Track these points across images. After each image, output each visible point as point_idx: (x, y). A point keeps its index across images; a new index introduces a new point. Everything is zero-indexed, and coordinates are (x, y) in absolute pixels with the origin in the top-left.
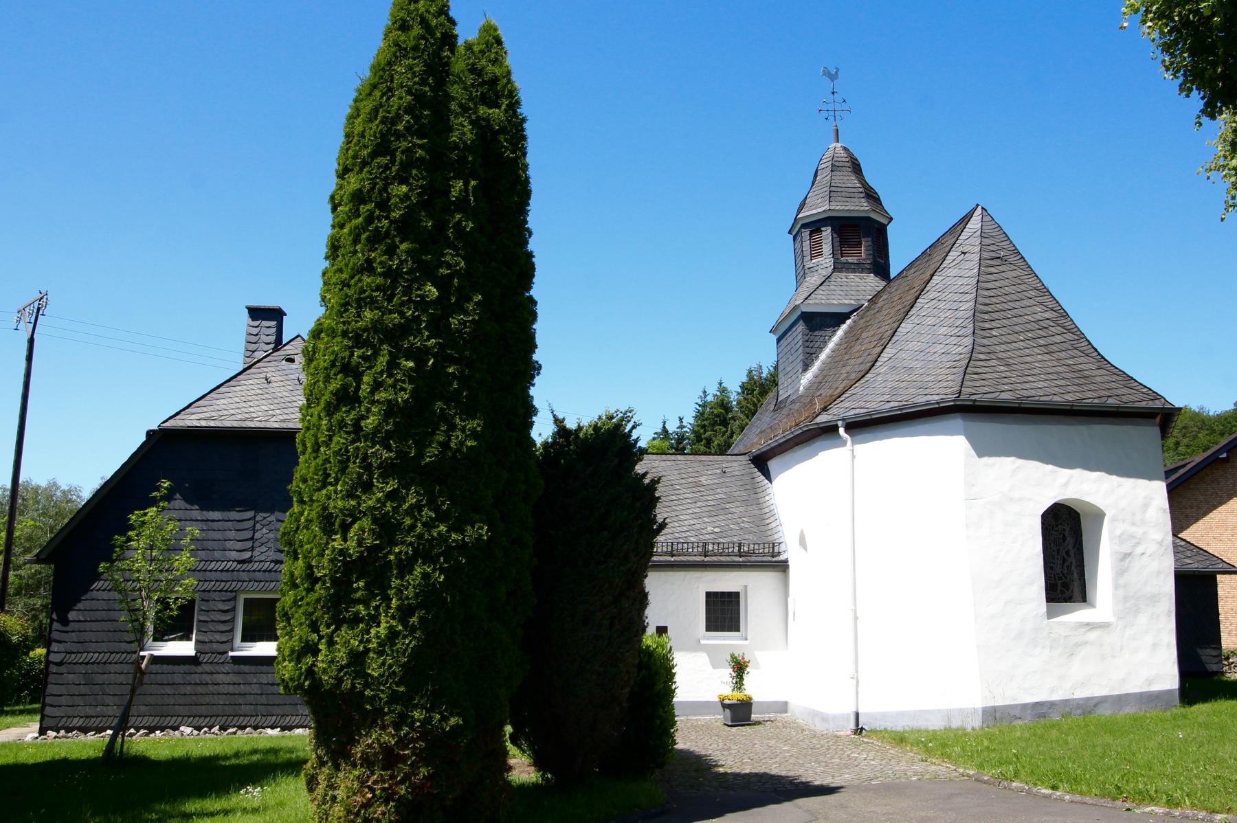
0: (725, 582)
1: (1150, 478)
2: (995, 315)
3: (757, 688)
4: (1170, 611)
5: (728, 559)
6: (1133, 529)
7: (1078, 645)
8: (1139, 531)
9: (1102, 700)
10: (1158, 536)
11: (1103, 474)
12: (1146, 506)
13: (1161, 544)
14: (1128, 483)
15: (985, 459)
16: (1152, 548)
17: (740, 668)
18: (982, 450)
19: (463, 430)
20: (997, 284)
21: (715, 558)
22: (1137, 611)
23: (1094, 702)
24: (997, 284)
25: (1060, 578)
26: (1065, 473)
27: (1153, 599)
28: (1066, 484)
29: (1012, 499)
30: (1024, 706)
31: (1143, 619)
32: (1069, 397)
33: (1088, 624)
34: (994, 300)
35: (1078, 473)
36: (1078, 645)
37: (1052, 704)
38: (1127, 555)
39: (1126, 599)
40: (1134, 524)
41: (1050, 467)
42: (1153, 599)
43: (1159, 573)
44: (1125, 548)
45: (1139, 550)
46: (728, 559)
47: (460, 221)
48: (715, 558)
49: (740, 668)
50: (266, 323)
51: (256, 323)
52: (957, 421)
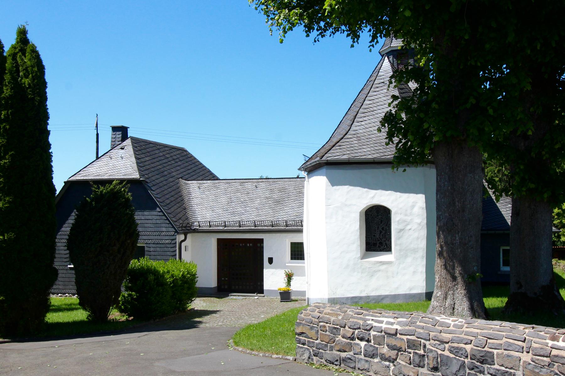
0: (296, 238)
1: (417, 193)
2: (367, 114)
3: (296, 285)
4: (423, 257)
5: (296, 228)
6: (406, 218)
7: (375, 272)
8: (408, 218)
9: (386, 297)
10: (419, 221)
11: (392, 192)
12: (413, 207)
13: (420, 224)
14: (406, 195)
15: (335, 187)
16: (415, 226)
17: (289, 277)
18: (334, 182)
19: (5, 200)
20: (376, 97)
21: (290, 228)
22: (406, 256)
23: (381, 298)
24: (376, 97)
25: (378, 240)
26: (373, 192)
27: (415, 251)
28: (373, 197)
29: (346, 205)
30: (348, 298)
31: (409, 260)
32: (375, 156)
33: (381, 262)
34: (370, 106)
35: (379, 192)
36: (375, 272)
37: (361, 298)
38: (401, 230)
39: (400, 250)
40: (406, 215)
41: (366, 189)
42: (415, 251)
43: (418, 238)
44: (401, 227)
45: (409, 227)
46: (296, 228)
47: (5, 126)
48: (290, 228)
49: (289, 277)
50: (118, 133)
51: (114, 133)
52: (324, 170)
